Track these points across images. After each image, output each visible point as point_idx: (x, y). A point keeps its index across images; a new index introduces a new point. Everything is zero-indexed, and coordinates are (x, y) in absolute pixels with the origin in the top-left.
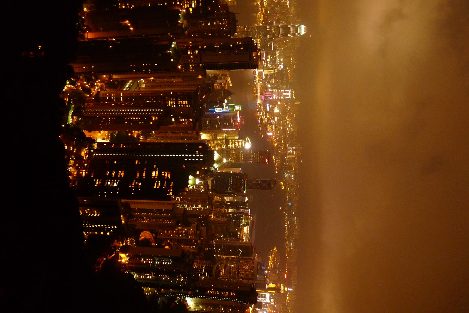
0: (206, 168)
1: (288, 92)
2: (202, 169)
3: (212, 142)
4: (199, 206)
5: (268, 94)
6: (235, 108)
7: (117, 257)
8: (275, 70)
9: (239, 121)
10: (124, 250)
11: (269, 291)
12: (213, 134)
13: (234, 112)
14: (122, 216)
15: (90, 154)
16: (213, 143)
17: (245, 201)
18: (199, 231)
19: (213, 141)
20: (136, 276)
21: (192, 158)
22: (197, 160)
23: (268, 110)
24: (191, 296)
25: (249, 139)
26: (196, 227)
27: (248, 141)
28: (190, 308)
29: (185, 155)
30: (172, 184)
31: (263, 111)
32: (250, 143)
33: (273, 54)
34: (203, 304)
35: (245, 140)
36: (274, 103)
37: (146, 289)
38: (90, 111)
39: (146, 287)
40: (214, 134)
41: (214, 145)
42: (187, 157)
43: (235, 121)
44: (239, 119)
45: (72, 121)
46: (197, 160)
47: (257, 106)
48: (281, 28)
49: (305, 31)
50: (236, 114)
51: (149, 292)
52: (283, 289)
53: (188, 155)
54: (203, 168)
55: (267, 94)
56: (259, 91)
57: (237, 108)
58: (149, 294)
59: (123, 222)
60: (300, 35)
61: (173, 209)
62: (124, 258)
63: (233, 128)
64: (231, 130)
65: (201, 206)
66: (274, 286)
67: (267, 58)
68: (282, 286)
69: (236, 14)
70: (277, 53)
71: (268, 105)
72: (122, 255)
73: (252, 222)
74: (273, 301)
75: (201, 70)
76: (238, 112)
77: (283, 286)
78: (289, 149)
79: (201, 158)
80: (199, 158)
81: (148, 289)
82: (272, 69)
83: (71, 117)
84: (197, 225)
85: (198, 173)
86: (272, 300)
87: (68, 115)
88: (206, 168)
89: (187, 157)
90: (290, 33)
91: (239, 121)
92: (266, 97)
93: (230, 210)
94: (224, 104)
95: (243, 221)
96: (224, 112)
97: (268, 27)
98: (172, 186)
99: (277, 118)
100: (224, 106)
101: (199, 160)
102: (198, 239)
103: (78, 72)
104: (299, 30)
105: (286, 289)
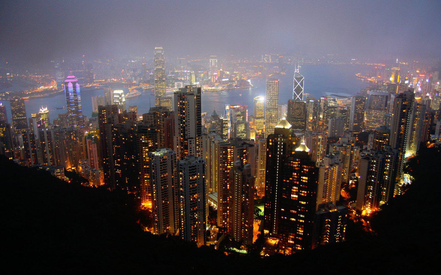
0: (290, 136)
1: (212, 61)
2: (291, 140)
3: (258, 131)
6: (227, 110)
7: (365, 218)
9: (240, 106)
10: (359, 212)
12: (251, 130)
13: (231, 111)
14: (330, 211)
15: (274, 237)
20: (382, 203)
21: (280, 148)
22: (282, 143)
23: (228, 79)
24: (405, 153)
26: (339, 147)
27: (257, 98)
28: (413, 154)
29: (278, 155)
32: (259, 96)
34: (410, 143)
35: (256, 101)
36: (222, 73)
37: (395, 193)
38: (235, 235)
39: (394, 192)
42: (280, 152)
43: (238, 110)
44: (238, 106)
45: (244, 249)
46: (282, 143)
48: (157, 67)
50: (234, 108)
51: (398, 191)
52: (396, 68)
53: (278, 151)
54: (290, 138)
56: (210, 88)
57: (227, 108)
58: (400, 191)
59: (336, 210)
62: (367, 211)
63: (246, 112)
64: (247, 113)
65: (319, 143)
67: (181, 81)
69: (152, 106)
70: (176, 71)
71: (223, 80)
72: (364, 213)
75: (202, 138)
76: (231, 107)
78: (264, 60)
79: (281, 139)
80: (281, 142)
81: (396, 191)
83: (241, 251)
84: (338, 146)
85: (294, 143)
87: (239, 253)
88: (290, 136)
89: (280, 152)
91: (240, 106)
92: (216, 82)
93: (321, 116)
94: (224, 120)
95: (332, 104)
96: (231, 120)
97: (156, 79)
98: (307, 166)
99: (235, 71)
100: (226, 119)
101: (282, 142)
102: (350, 146)
103: (203, 242)
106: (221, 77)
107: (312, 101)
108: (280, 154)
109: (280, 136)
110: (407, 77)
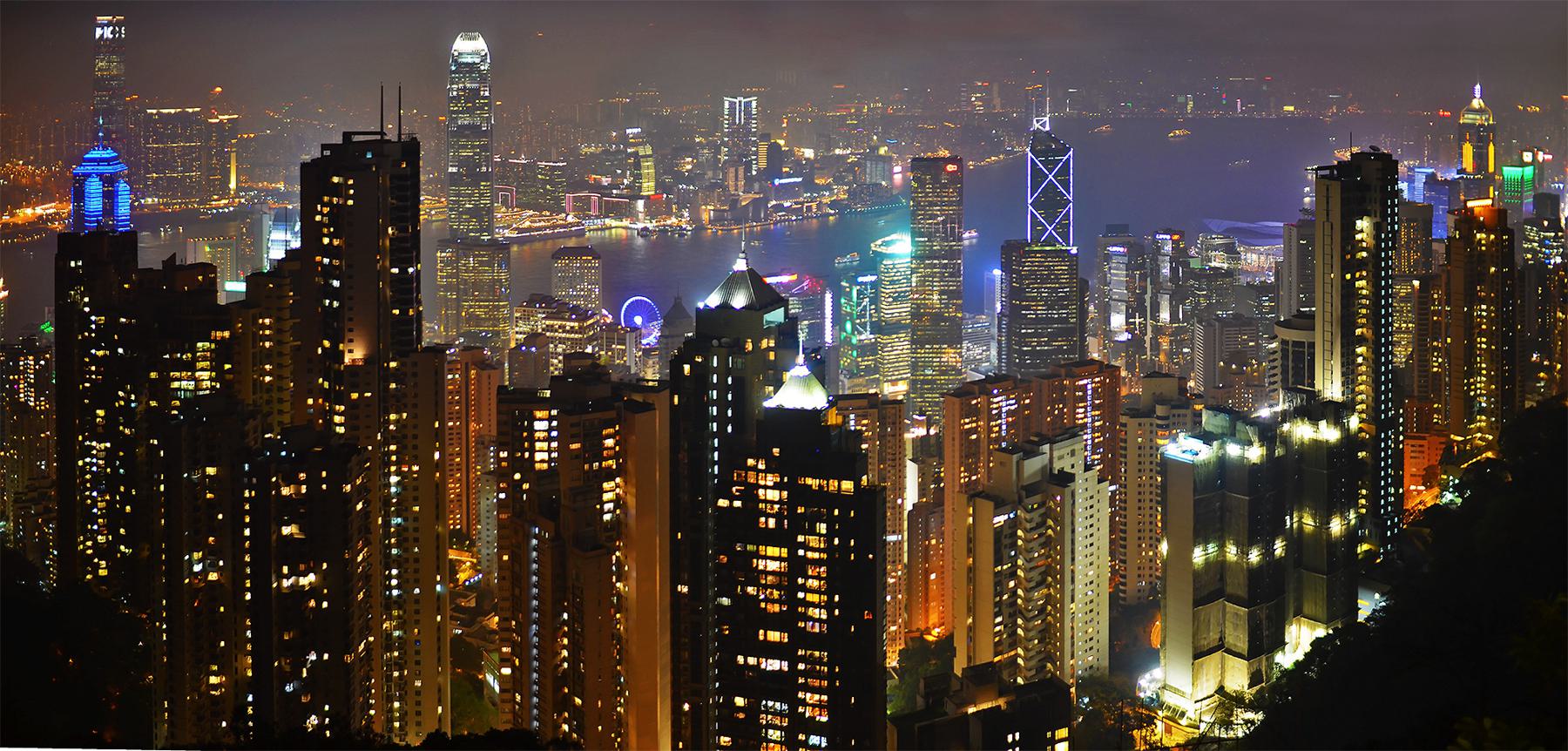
4: (1079, 416)
5: (737, 179)
8: (642, 157)
9: (794, 277)
11: (1491, 169)
16: (894, 382)
17: (1123, 255)
18: (1155, 407)
19: (886, 384)
21: (722, 403)
25: (879, 242)
27: (886, 244)
29: (714, 435)
30: (809, 481)
31: (801, 199)
32: (893, 237)
33: (596, 164)
40: (845, 377)
41: (902, 379)
47: (780, 221)
49: (474, 38)
52: (1478, 117)
53: (714, 419)
55: (737, 179)
60: (486, 54)
61: (988, 497)
66: (1468, 149)
68: (1466, 121)
71: (777, 182)
73: (1226, 233)
74: (1530, 154)
77: (1466, 116)
80: (724, 371)
82: (637, 166)
86: (1528, 157)
90: (478, 90)
91: (794, 277)
101: (728, 372)
104: (469, 60)
105: (1477, 103)
106: (773, 170)
107: (1121, 249)
108: (721, 430)
109: (720, 345)
110: (1525, 154)
